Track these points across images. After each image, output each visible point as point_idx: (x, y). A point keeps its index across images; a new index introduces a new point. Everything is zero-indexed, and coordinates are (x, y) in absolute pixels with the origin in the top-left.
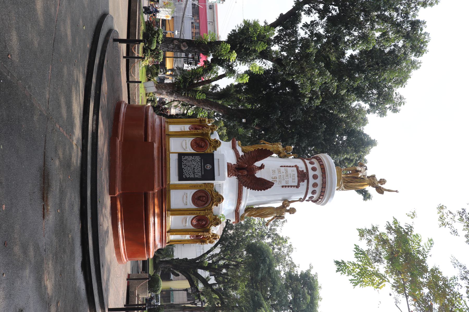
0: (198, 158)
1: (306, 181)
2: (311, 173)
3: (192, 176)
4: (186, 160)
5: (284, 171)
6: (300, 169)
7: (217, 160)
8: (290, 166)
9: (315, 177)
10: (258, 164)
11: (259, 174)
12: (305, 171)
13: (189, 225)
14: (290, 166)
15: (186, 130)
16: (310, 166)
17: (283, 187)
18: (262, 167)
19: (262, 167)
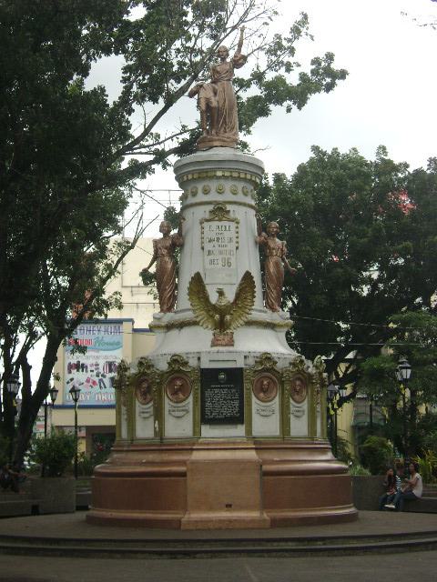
0: (208, 393)
1: (229, 207)
2: (213, 197)
3: (237, 403)
4: (212, 412)
5: (212, 244)
6: (207, 216)
7: (211, 363)
8: (203, 233)
9: (220, 192)
10: (214, 298)
11: (230, 296)
12: (211, 207)
13: (305, 406)
14: (203, 233)
15: (152, 409)
16: (201, 197)
17: (237, 248)
18: (221, 293)
19: (221, 293)
